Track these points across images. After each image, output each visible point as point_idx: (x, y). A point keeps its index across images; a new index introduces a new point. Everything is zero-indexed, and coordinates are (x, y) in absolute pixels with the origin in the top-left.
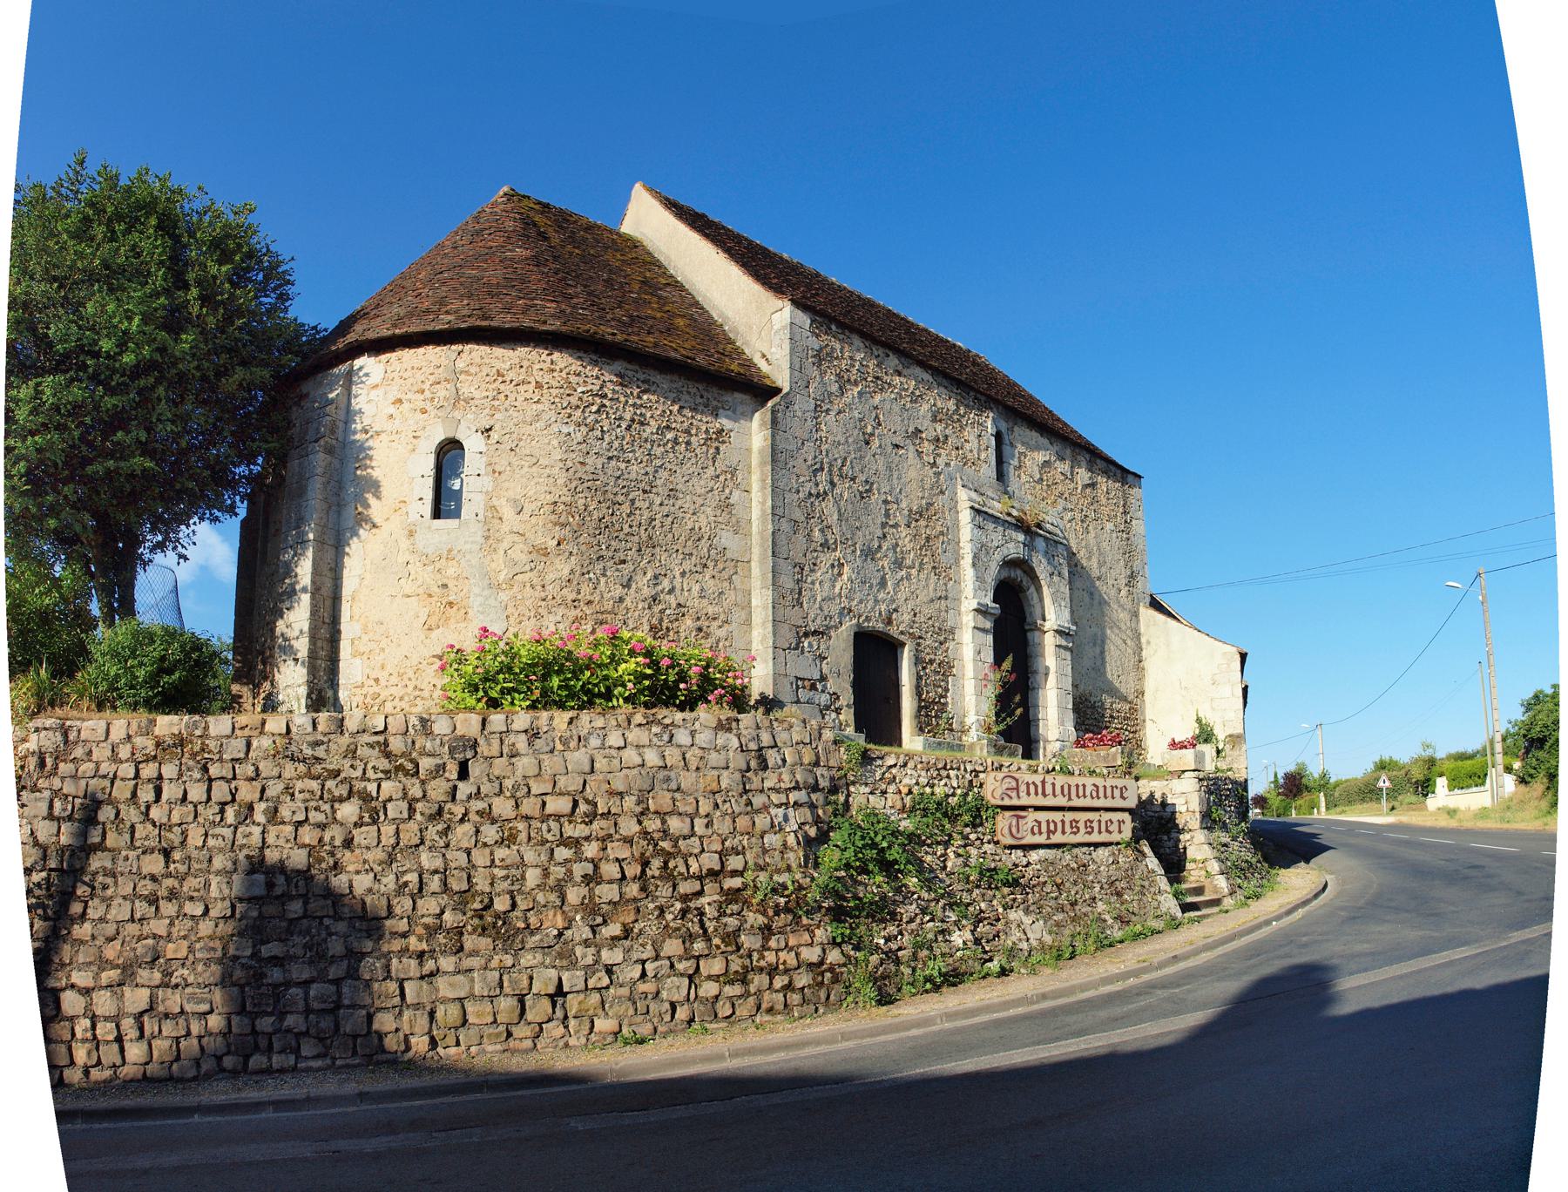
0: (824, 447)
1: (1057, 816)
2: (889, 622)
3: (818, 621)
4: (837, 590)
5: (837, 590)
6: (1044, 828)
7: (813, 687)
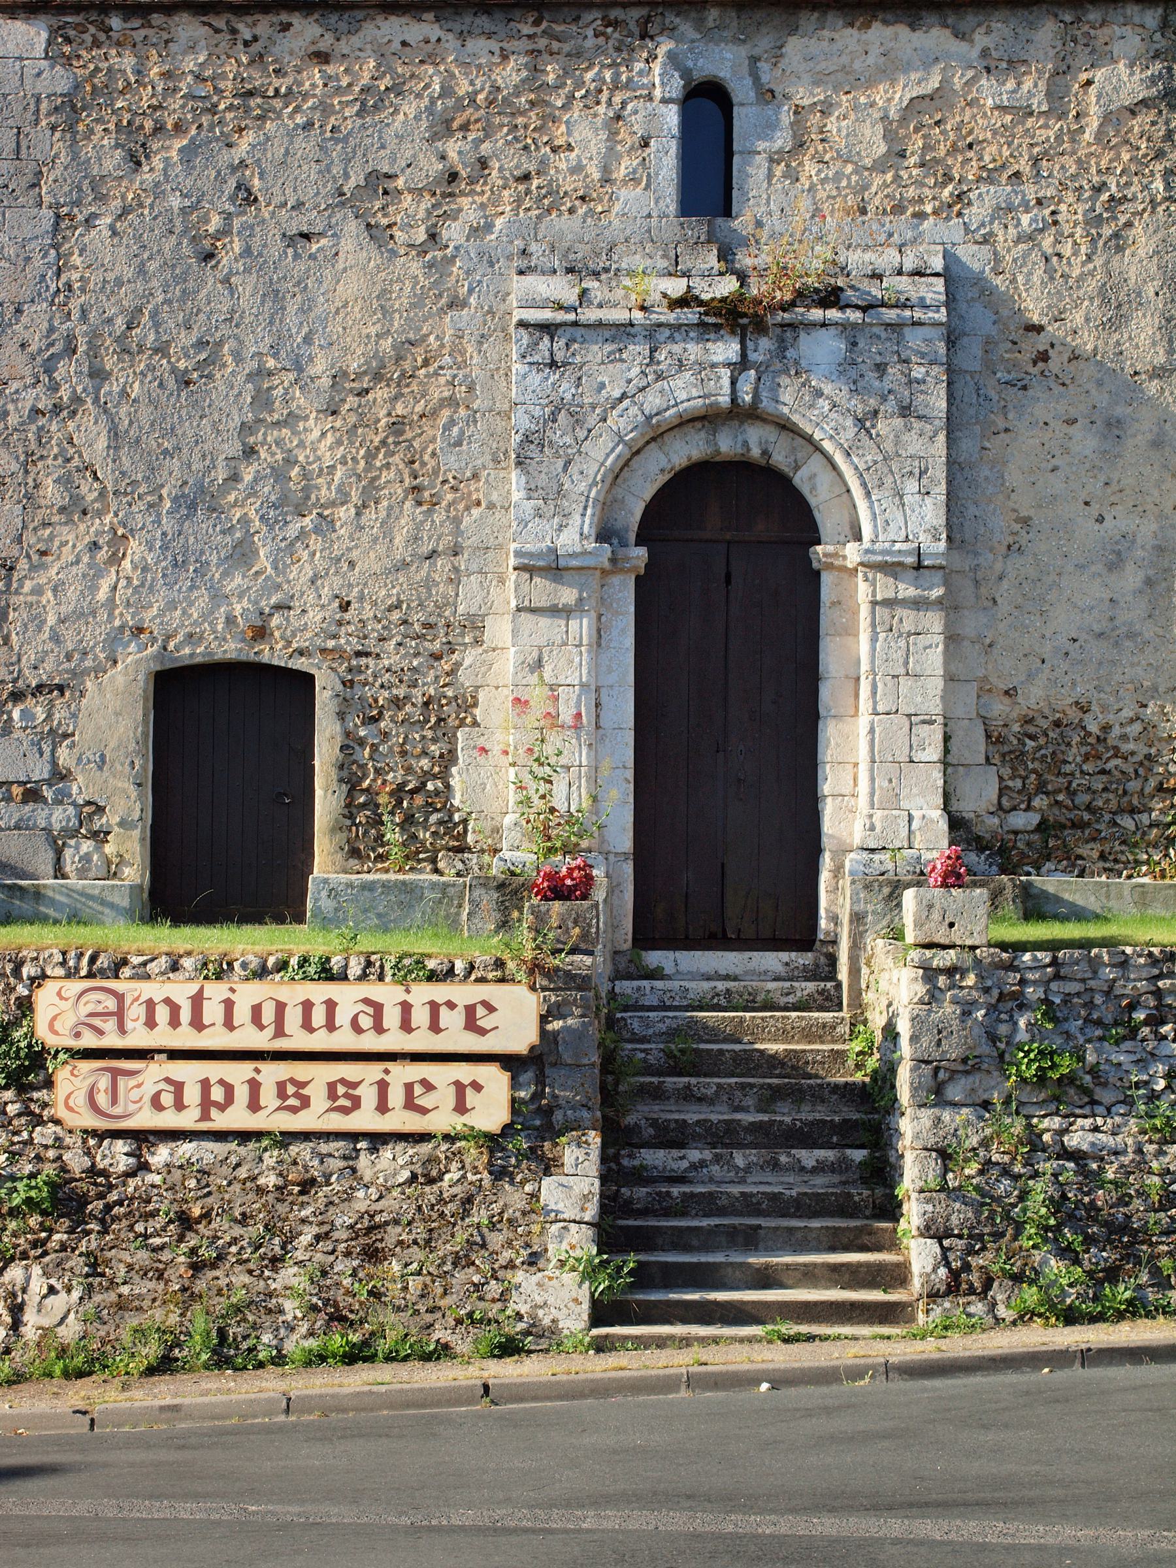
0: (75, 305)
2: (261, 633)
3: (49, 665)
4: (102, 594)
5: (102, 594)
7: (32, 795)
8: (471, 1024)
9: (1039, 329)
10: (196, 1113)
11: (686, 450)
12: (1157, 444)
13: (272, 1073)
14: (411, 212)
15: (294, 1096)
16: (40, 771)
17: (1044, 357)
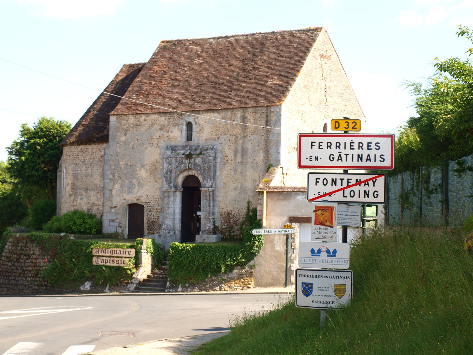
1: (108, 259)
6: (104, 261)
8: (129, 254)
9: (227, 156)
10: (104, 264)
11: (186, 174)
12: (241, 173)
13: (112, 259)
14: (155, 142)
15: (113, 261)
16: (115, 218)
17: (228, 160)
